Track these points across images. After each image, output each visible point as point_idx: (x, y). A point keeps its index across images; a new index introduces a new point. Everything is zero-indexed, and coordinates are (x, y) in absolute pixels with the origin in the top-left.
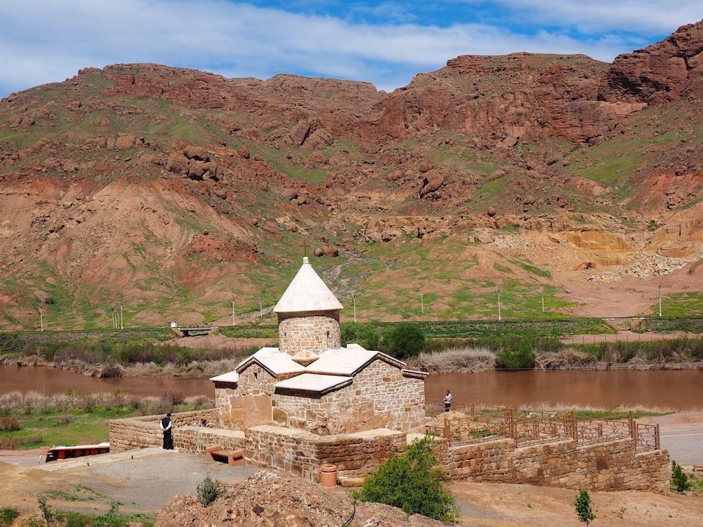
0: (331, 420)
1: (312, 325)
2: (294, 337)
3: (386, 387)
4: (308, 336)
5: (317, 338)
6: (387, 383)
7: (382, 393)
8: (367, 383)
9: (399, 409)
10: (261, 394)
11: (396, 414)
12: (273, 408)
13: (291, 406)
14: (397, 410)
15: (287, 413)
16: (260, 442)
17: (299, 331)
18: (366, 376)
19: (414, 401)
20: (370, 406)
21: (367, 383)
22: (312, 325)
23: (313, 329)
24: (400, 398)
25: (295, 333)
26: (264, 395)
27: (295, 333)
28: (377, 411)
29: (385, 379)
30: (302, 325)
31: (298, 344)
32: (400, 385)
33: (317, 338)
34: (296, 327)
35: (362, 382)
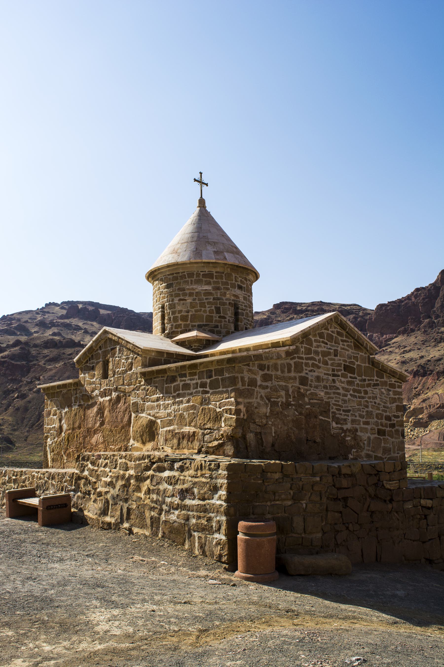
0: (252, 426)
3: (349, 383)
5: (218, 310)
6: (349, 375)
7: (341, 391)
8: (319, 367)
9: (369, 427)
11: (364, 436)
14: (366, 430)
18: (317, 353)
19: (388, 418)
20: (326, 412)
21: (319, 367)
24: (370, 409)
25: (180, 300)
28: (334, 425)
29: (346, 368)
30: (195, 287)
32: (369, 385)
33: (218, 310)
34: (184, 290)
35: (310, 362)
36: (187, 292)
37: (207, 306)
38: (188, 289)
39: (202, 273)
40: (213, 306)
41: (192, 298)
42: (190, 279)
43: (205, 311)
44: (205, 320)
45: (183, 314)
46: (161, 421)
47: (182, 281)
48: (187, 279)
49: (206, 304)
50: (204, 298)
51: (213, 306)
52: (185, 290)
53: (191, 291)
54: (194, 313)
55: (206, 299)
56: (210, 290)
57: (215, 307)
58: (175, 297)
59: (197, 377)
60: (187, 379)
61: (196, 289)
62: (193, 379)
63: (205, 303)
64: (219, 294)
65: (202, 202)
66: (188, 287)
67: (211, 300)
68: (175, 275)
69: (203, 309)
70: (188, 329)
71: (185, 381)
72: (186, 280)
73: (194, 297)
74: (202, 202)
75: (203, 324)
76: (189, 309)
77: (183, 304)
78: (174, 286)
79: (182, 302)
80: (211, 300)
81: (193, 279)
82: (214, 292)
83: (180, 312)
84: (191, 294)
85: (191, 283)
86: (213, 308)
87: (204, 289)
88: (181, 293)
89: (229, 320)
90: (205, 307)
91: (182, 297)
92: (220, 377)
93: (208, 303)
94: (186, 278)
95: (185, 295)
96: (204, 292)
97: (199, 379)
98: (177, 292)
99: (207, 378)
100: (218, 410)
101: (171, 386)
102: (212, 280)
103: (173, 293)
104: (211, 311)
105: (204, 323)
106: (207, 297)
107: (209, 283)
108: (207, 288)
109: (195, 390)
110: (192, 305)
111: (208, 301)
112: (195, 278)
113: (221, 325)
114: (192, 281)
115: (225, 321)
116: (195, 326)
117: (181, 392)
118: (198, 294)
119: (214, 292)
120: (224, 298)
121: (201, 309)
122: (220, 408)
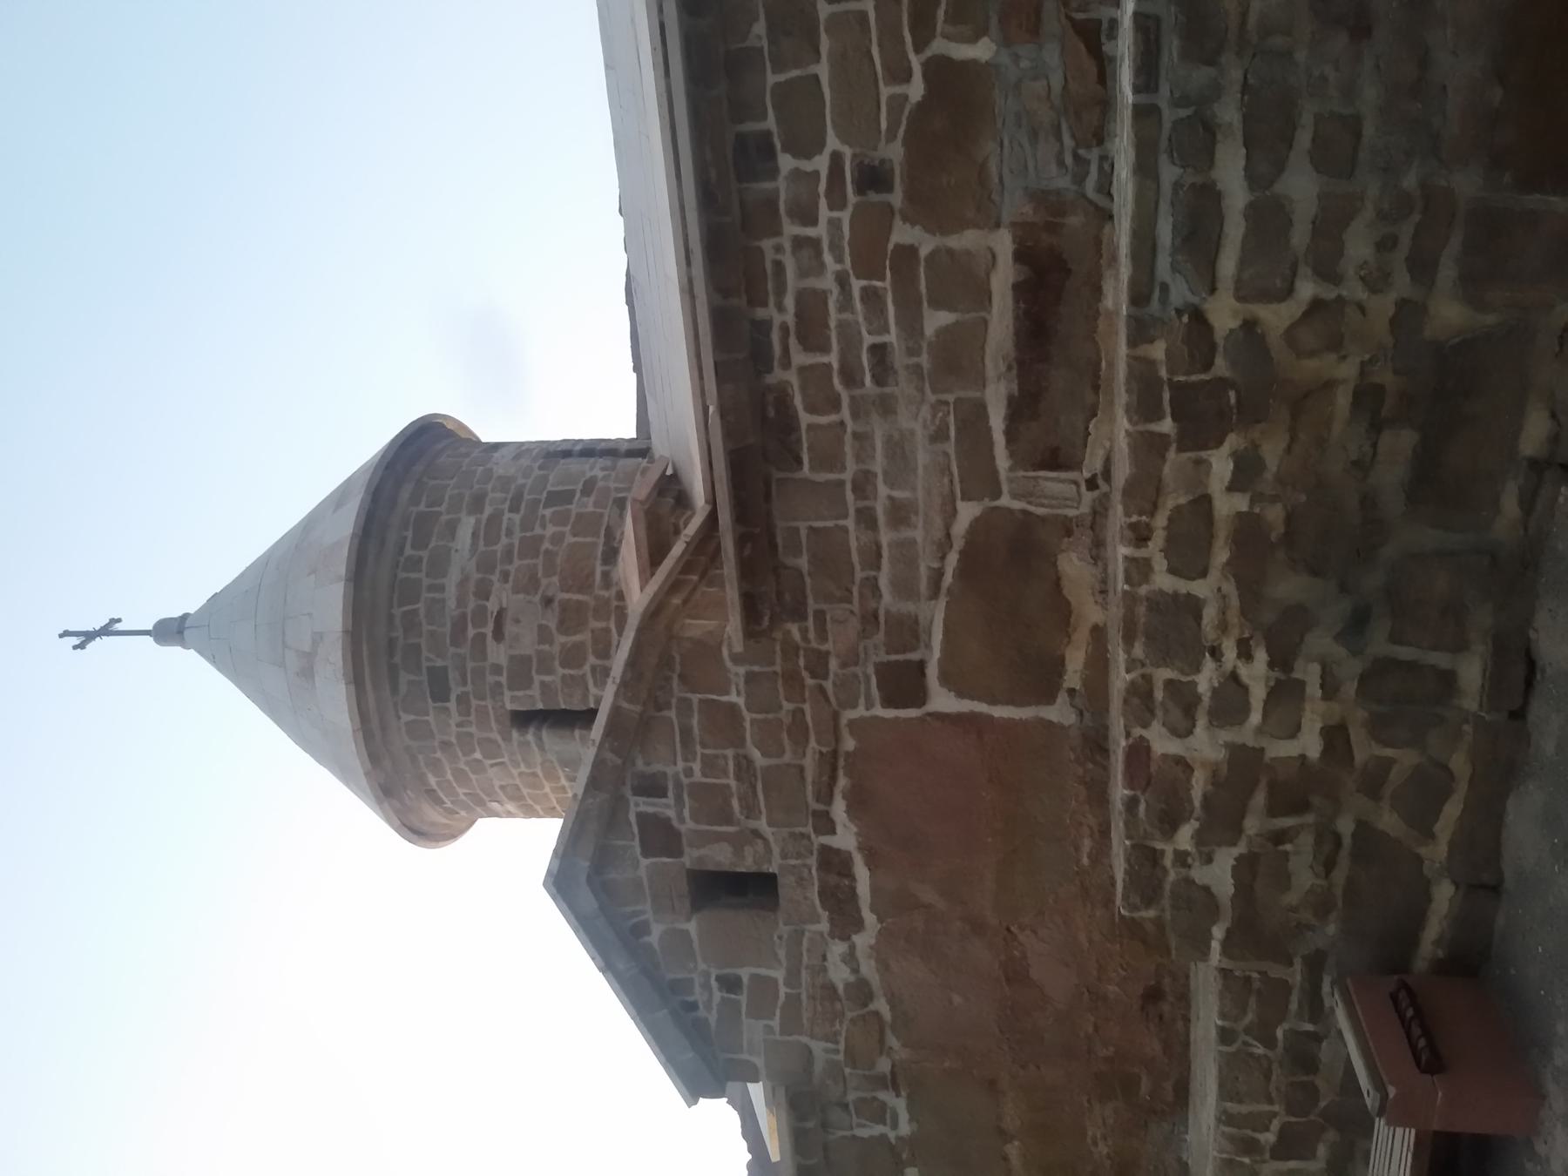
1: (467, 525)
2: (528, 644)
4: (531, 546)
10: (845, 838)
12: (943, 701)
13: (898, 450)
15: (967, 512)
16: (1248, 732)
17: (492, 606)
22: (467, 525)
23: (495, 519)
25: (498, 634)
26: (858, 804)
27: (498, 634)
31: (571, 618)
34: (459, 627)
36: (472, 603)
37: (538, 531)
38: (461, 602)
39: (408, 551)
40: (541, 511)
41: (497, 585)
42: (425, 595)
43: (557, 539)
44: (589, 540)
45: (553, 625)
46: (966, 497)
47: (426, 627)
48: (421, 606)
49: (528, 534)
50: (504, 540)
51: (541, 511)
52: (464, 616)
53: (472, 587)
54: (555, 579)
55: (509, 533)
56: (478, 522)
57: (545, 507)
58: (485, 659)
59: (767, 244)
60: (777, 319)
61: (463, 570)
62: (779, 267)
63: (522, 540)
64: (499, 495)
65: (170, 631)
66: (452, 603)
67: (517, 518)
68: (397, 659)
69: (546, 545)
70: (615, 603)
71: (785, 329)
72: (422, 612)
73: (495, 578)
74: (170, 631)
75: (605, 544)
76: (537, 599)
77: (517, 621)
78: (439, 663)
79: (509, 629)
80: (517, 518)
81: (426, 582)
82: (488, 510)
83: (544, 635)
84: (484, 592)
85: (442, 588)
86: (548, 512)
87: (468, 541)
88: (471, 632)
89: (603, 469)
90: (541, 538)
91: (489, 630)
92: (772, 79)
93: (527, 525)
94: (415, 612)
95: (481, 612)
96: (481, 543)
97: (777, 232)
98: (465, 650)
99: (773, 173)
100: (916, 90)
101: (810, 427)
102: (444, 518)
103: (470, 665)
104: (560, 519)
105: (602, 540)
106: (503, 532)
107: (452, 529)
108: (470, 531)
109: (828, 258)
110: (530, 584)
111: (517, 529)
112: (422, 575)
113: (618, 490)
114: (431, 588)
115: (605, 478)
116: (606, 576)
117: (833, 359)
118: (486, 565)
119: (488, 510)
120: (521, 481)
121: (547, 552)
122: (907, 77)
